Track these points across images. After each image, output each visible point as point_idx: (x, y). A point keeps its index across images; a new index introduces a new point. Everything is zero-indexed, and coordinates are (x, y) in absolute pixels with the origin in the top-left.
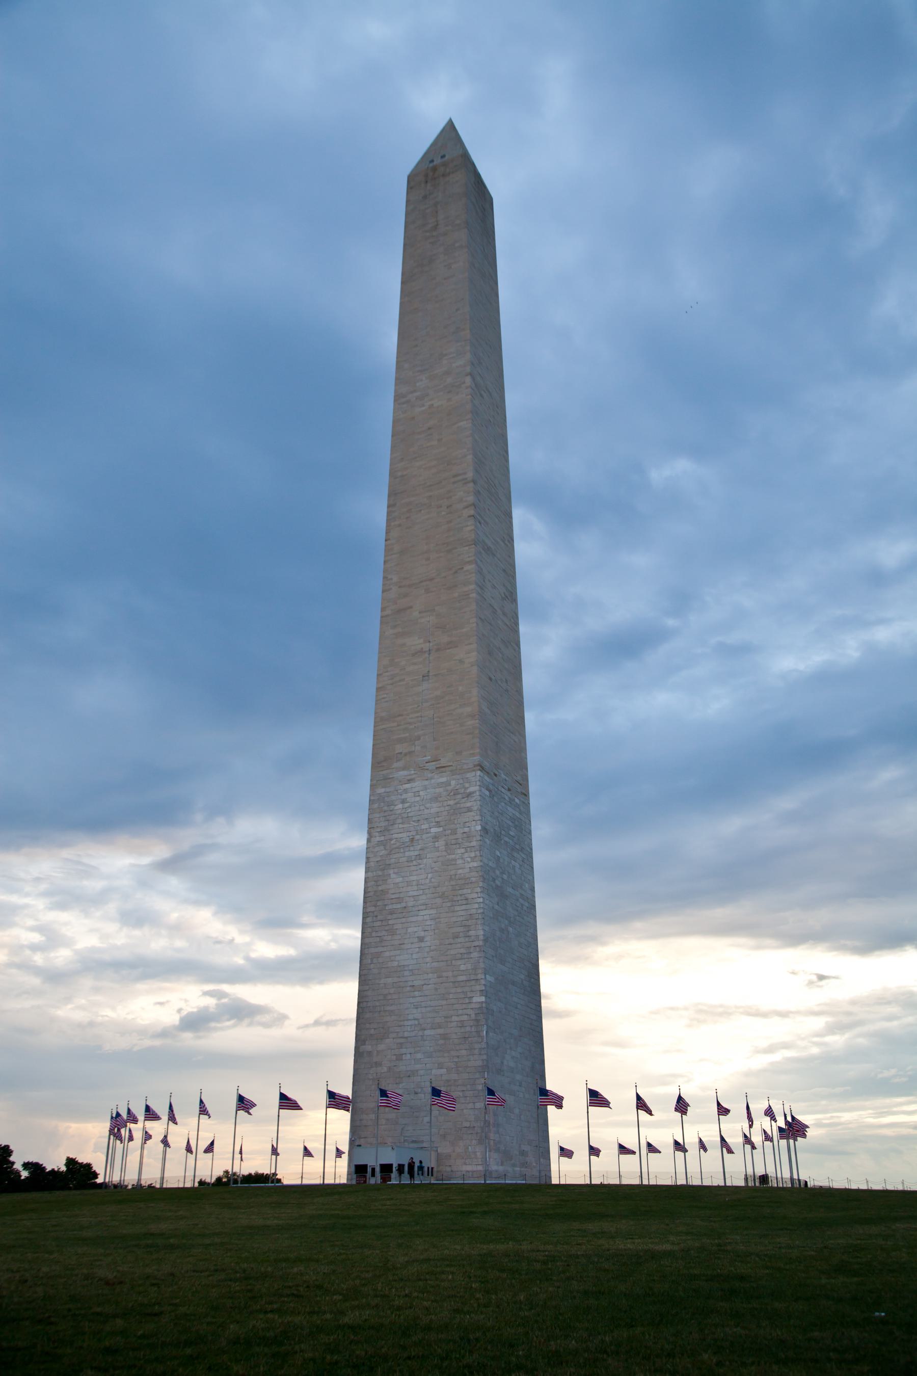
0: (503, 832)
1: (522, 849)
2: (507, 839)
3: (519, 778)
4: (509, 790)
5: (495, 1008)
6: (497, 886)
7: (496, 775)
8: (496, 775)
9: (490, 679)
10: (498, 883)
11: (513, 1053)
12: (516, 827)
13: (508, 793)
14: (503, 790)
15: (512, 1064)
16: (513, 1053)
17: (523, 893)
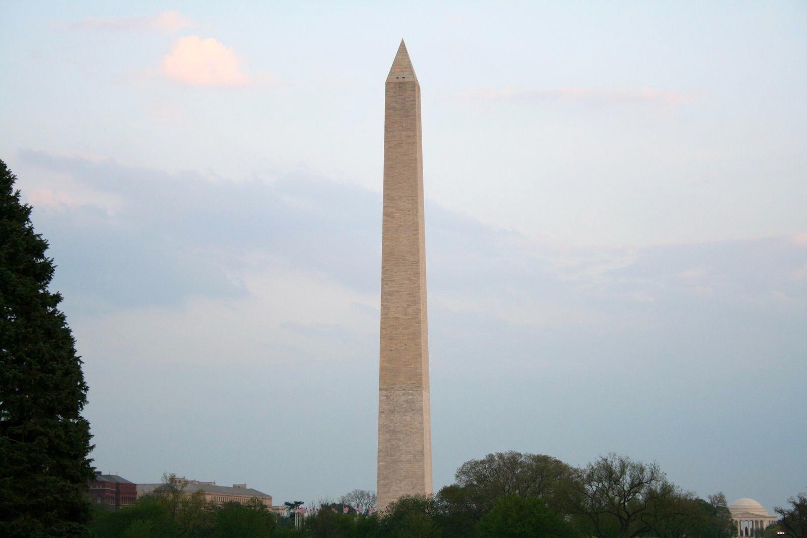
0: (397, 408)
1: (413, 410)
3: (413, 382)
4: (403, 390)
5: (385, 473)
6: (390, 430)
7: (392, 388)
8: (392, 388)
10: (390, 428)
11: (398, 485)
12: (408, 403)
13: (403, 392)
14: (399, 392)
15: (398, 489)
16: (398, 485)
17: (413, 426)
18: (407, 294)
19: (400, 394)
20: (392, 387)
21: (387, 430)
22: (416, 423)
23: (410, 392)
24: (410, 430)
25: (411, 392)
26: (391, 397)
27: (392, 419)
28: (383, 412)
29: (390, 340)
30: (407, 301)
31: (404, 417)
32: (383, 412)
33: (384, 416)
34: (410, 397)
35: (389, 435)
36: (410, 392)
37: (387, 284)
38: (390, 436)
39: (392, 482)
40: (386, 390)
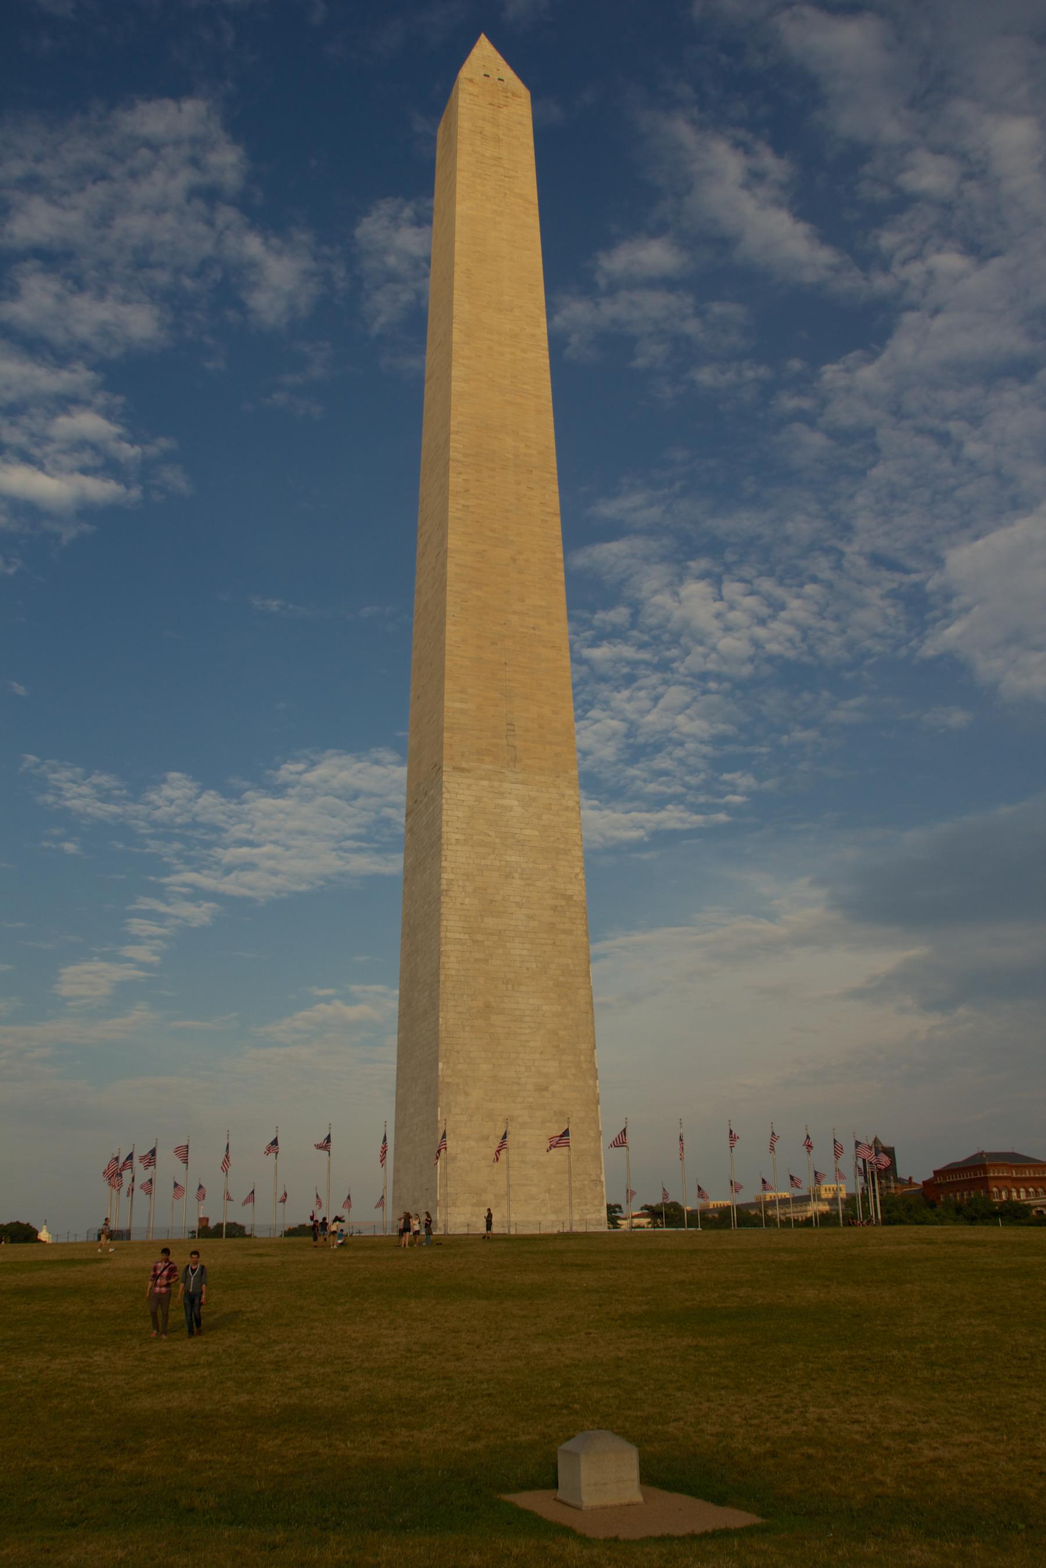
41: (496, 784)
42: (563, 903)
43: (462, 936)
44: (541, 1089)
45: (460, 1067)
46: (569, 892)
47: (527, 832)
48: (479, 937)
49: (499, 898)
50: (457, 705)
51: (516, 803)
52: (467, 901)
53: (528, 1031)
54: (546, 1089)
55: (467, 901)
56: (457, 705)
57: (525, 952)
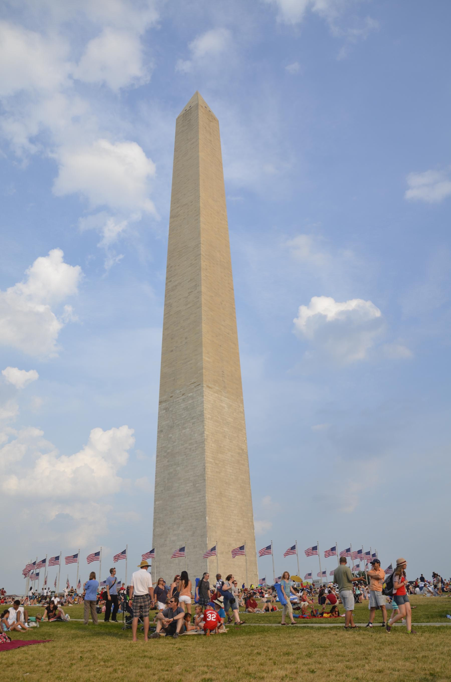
1: (193, 418)
2: (179, 422)
4: (183, 395)
9: (172, 351)
13: (183, 397)
14: (178, 399)
18: (189, 282)
19: (180, 401)
20: (171, 395)
21: (166, 454)
22: (196, 435)
23: (189, 395)
24: (189, 447)
25: (191, 394)
26: (170, 409)
27: (171, 438)
28: (162, 431)
29: (172, 339)
30: (188, 289)
31: (184, 431)
32: (162, 431)
33: (162, 436)
34: (190, 402)
35: (167, 460)
36: (189, 395)
37: (171, 281)
38: (168, 461)
39: (169, 529)
40: (165, 401)
41: (220, 396)
42: (241, 452)
43: (211, 460)
44: (238, 532)
45: (213, 519)
46: (243, 448)
47: (230, 419)
48: (217, 462)
49: (222, 446)
50: (207, 359)
51: (226, 406)
52: (213, 445)
53: (233, 506)
54: (239, 532)
55: (213, 445)
56: (207, 359)
57: (231, 471)
